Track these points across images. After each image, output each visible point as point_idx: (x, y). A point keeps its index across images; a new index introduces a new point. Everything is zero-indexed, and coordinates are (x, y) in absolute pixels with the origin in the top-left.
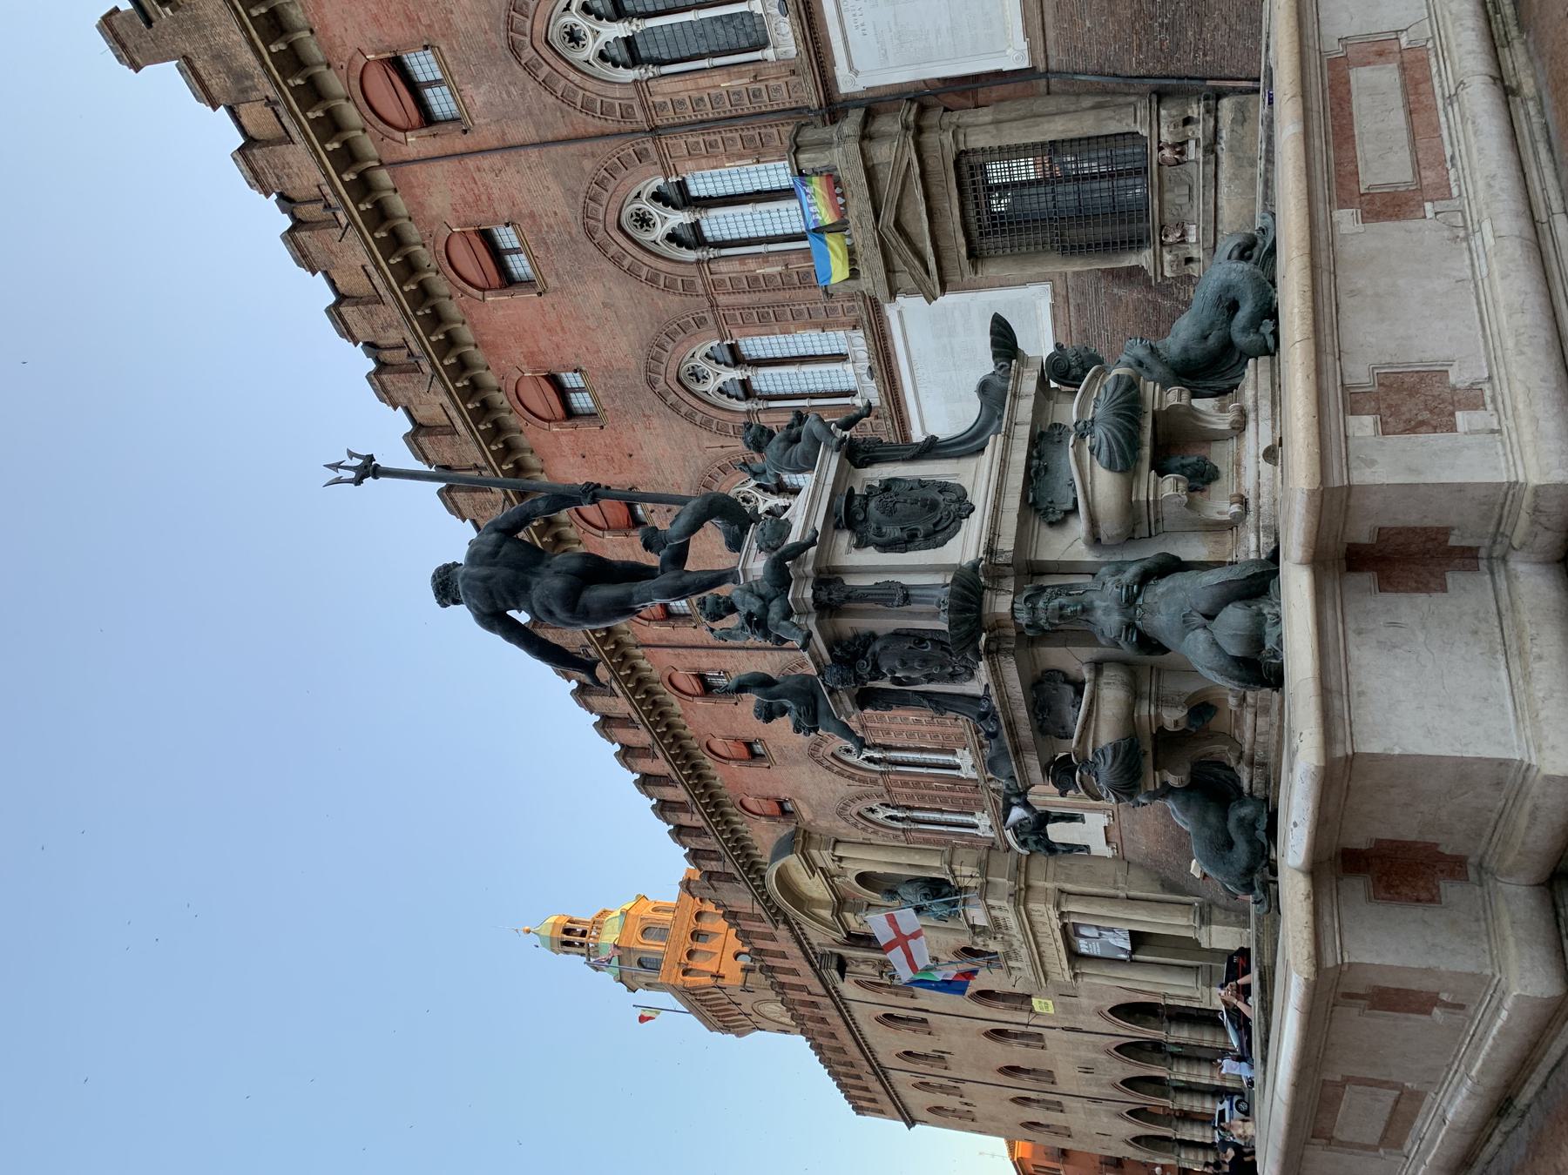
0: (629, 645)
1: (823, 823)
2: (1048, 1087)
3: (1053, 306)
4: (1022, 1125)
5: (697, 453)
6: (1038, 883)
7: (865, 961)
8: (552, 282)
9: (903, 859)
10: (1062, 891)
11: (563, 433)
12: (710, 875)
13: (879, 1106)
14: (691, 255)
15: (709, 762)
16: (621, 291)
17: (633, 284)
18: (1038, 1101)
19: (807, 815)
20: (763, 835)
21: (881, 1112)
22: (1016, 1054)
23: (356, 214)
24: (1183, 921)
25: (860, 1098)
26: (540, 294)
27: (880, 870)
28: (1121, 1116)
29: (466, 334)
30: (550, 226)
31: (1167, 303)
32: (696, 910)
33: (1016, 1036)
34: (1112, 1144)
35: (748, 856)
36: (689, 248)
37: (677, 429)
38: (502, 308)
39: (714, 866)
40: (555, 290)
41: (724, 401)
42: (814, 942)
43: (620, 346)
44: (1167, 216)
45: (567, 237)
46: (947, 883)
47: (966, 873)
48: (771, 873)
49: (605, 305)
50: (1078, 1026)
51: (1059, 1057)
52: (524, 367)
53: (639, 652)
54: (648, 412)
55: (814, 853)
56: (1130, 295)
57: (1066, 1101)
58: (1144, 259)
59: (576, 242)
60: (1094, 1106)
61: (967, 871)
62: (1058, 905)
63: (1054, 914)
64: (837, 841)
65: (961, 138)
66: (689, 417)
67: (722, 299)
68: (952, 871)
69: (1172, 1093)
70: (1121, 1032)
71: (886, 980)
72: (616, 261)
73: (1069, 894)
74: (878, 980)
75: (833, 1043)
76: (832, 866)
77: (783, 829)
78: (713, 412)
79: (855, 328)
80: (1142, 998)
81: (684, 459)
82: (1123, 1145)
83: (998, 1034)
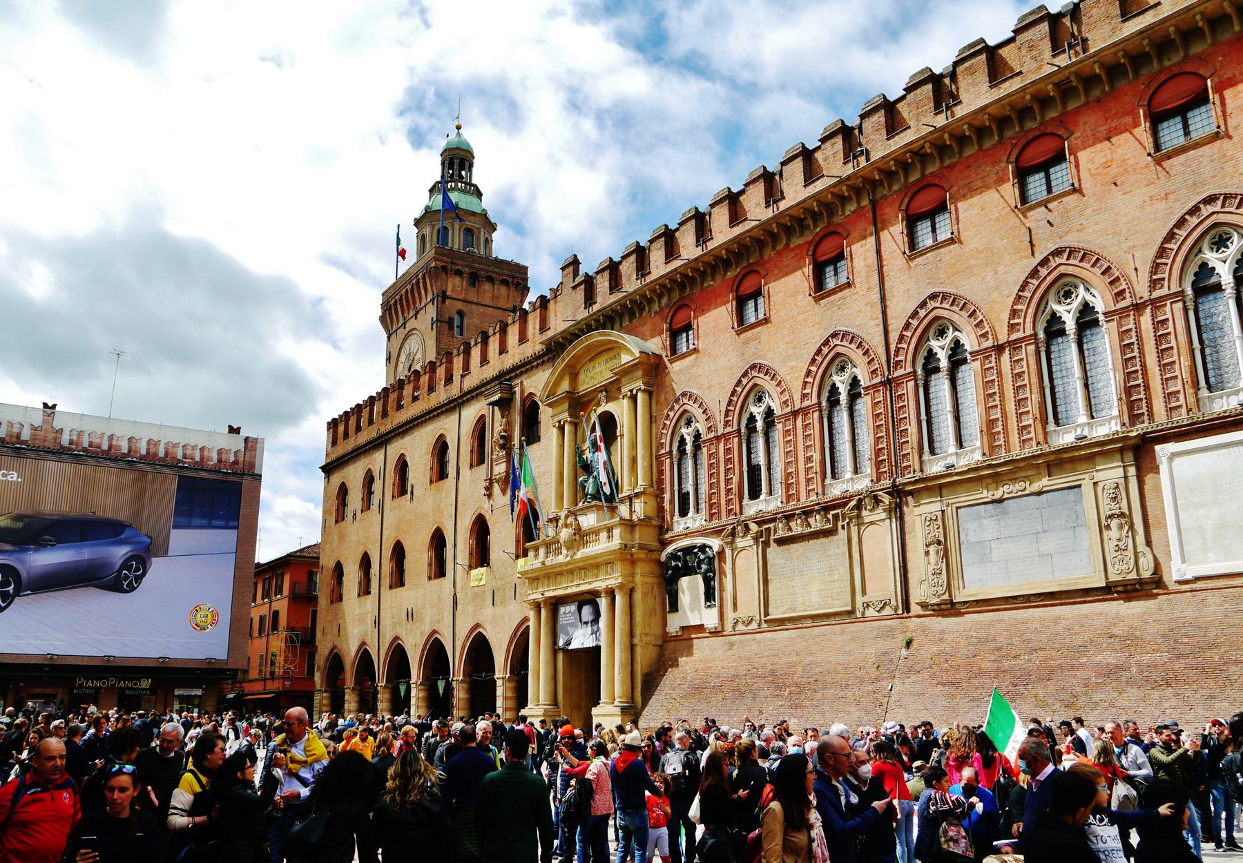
2: (386, 581)
10: (632, 590)
12: (589, 282)
13: (340, 440)
21: (334, 442)
24: (618, 690)
39: (603, 284)
54: (1171, 197)
57: (371, 600)
62: (621, 586)
70: (459, 644)
73: (631, 596)
82: (330, 646)
83: (438, 541)
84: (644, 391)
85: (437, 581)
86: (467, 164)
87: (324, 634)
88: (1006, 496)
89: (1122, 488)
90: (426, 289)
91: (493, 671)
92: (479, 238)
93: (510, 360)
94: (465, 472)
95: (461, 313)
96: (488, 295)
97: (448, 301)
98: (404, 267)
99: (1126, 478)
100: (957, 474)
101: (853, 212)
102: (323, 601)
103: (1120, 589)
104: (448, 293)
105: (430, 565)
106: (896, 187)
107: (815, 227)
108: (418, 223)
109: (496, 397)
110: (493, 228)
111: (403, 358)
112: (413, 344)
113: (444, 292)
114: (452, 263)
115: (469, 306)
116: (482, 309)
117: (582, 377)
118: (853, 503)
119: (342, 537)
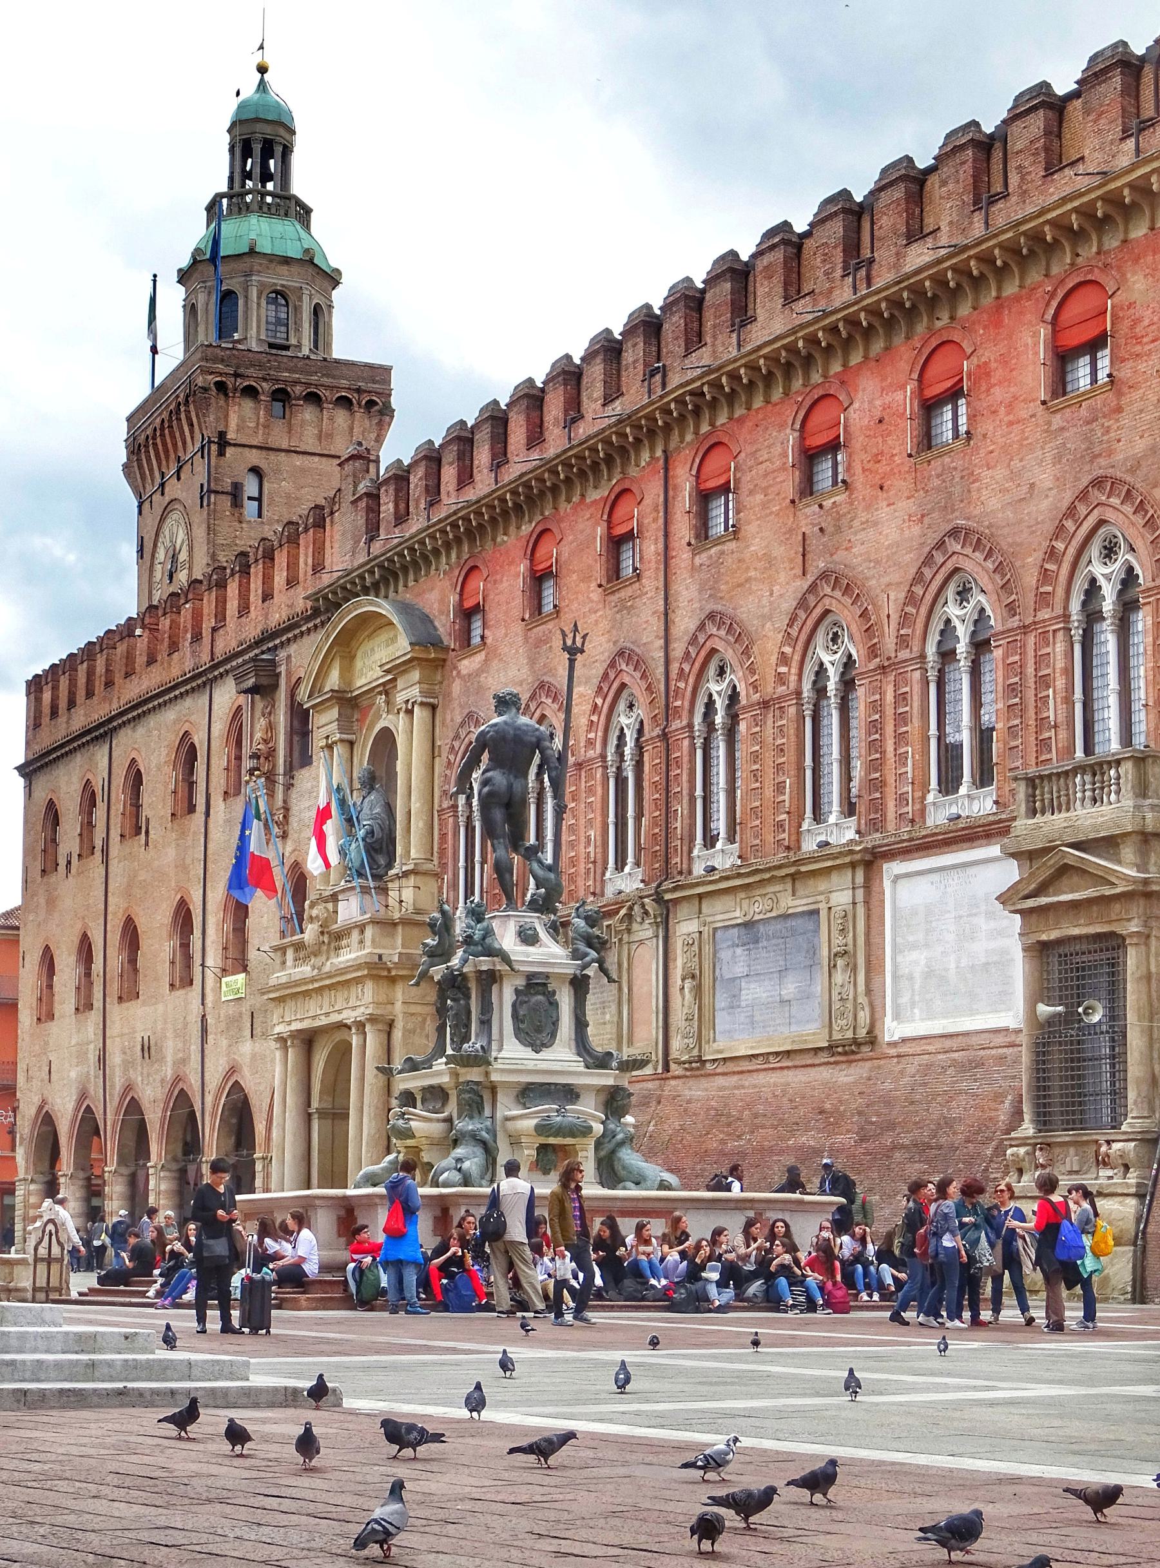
0: (666, 445)
1: (456, 687)
2: (114, 988)
3: (1007, 1030)
4: (47, 947)
5: (885, 580)
6: (400, 993)
7: (271, 727)
8: (1057, 421)
9: (415, 806)
10: (391, 1024)
11: (905, 399)
13: (46, 720)
14: (1075, 606)
15: (526, 529)
16: (1044, 509)
17: (1050, 527)
18: (88, 974)
19: (467, 665)
20: (437, 595)
22: (158, 948)
23: (1118, 183)
25: (55, 688)
26: (1044, 403)
27: (400, 766)
28: (83, 1096)
29: (1011, 289)
30: (1107, 431)
31: (989, 1152)
32: (321, 392)
33: (185, 946)
34: (36, 1084)
35: (405, 569)
36: (1084, 604)
37: (908, 558)
38: (1033, 343)
39: (387, 508)
40: (1049, 423)
41: (937, 626)
42: (293, 649)
43: (991, 501)
44: (1057, 1150)
45: (1097, 450)
46: (390, 865)
47: (405, 895)
48: (384, 608)
49: (1032, 485)
50: (210, 1038)
51: (160, 1008)
52: (974, 360)
53: (659, 453)
54: (926, 520)
55: (416, 675)
56: (1003, 1114)
57: (95, 1016)
58: (1027, 1128)
59: (1091, 462)
60: (92, 1057)
61: (408, 895)
62: (372, 1019)
63: (359, 1014)
64: (433, 708)
65: (1135, 940)
66: (918, 578)
67: (1031, 640)
68: (406, 874)
69: (125, 1171)
70: (209, 1099)
71: (247, 764)
72: (1071, 512)
73: (389, 1034)
74: (246, 751)
75: (141, 660)
76: (400, 698)
77: (445, 626)
78: (924, 610)
79: (996, 802)
80: (260, 1128)
81: (878, 562)
82: (37, 1100)
83: (183, 918)
84: (422, 704)
85: (180, 993)
86: (278, 150)
87: (28, 1079)
88: (757, 917)
89: (850, 917)
90: (191, 425)
91: (253, 1147)
92: (298, 309)
93: (278, 614)
94: (219, 806)
95: (256, 471)
96: (310, 433)
97: (230, 451)
98: (167, 365)
99: (854, 903)
100: (711, 882)
101: (648, 464)
102: (26, 1016)
103: (840, 1049)
104: (230, 436)
105: (173, 963)
106: (689, 437)
107: (610, 480)
108: (184, 277)
109: (251, 682)
110: (333, 279)
111: (161, 555)
112: (175, 532)
113: (222, 435)
114: (236, 375)
115: (272, 456)
116: (298, 461)
117: (359, 664)
118: (623, 912)
119: (51, 902)
